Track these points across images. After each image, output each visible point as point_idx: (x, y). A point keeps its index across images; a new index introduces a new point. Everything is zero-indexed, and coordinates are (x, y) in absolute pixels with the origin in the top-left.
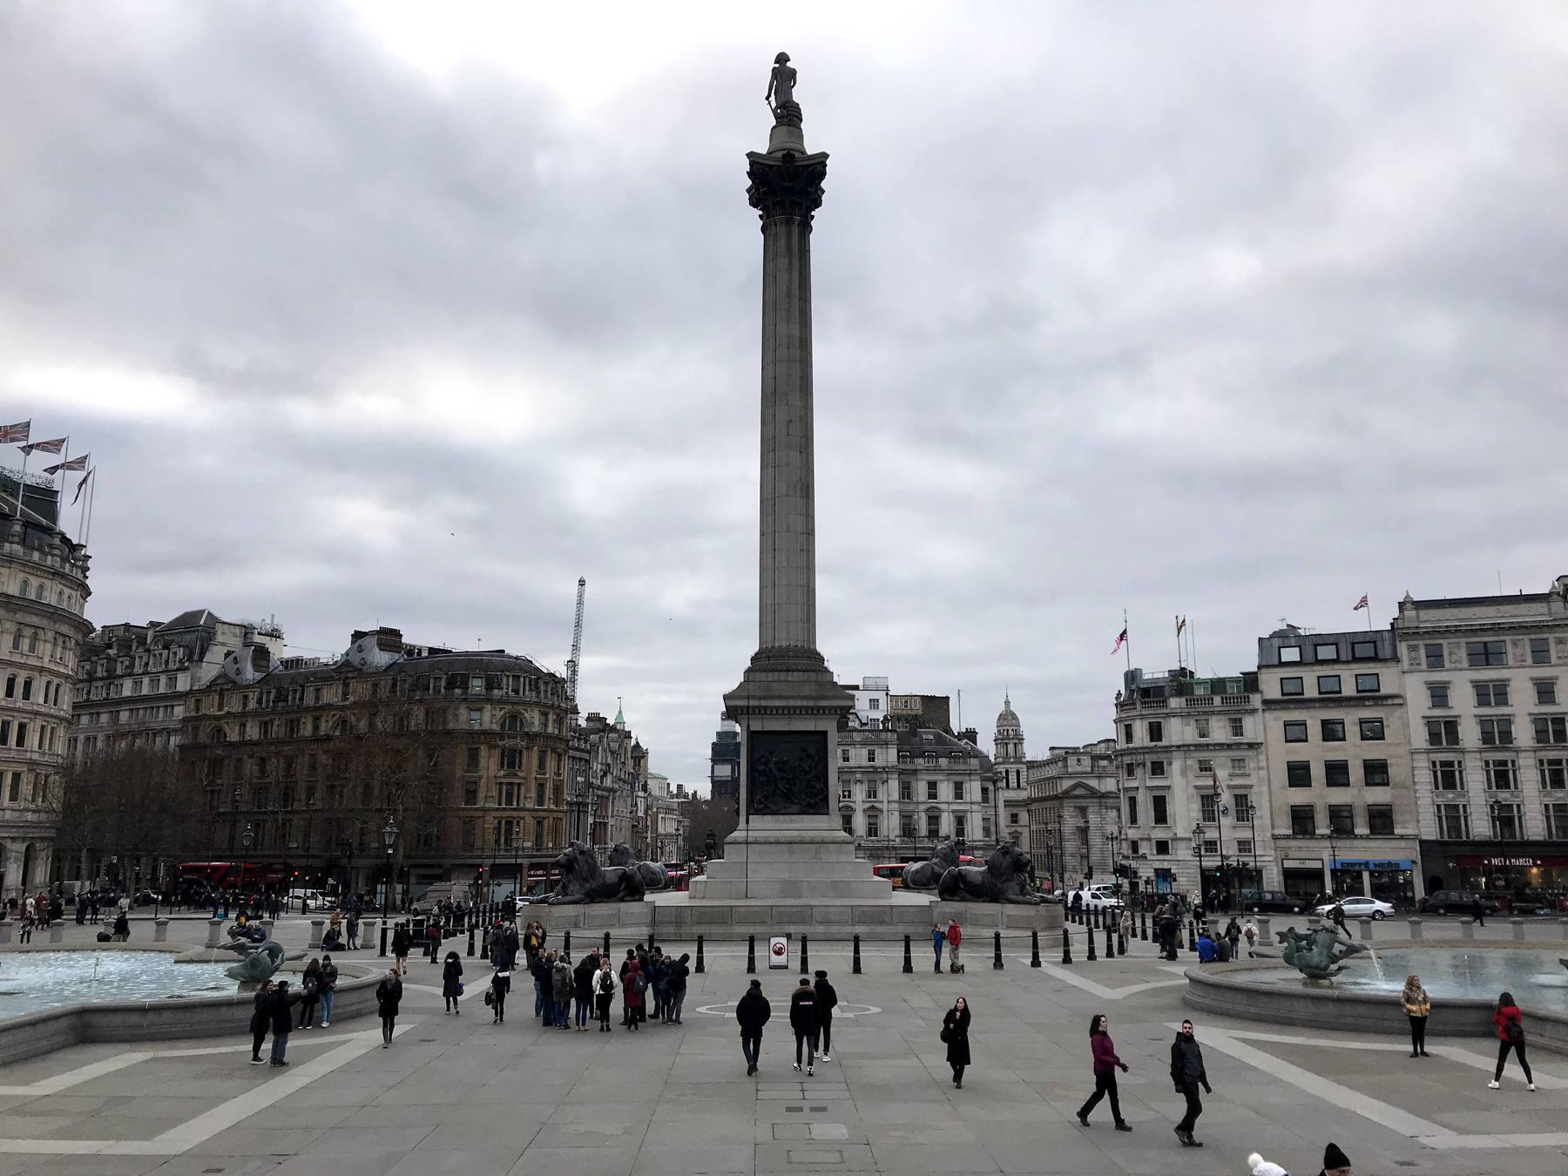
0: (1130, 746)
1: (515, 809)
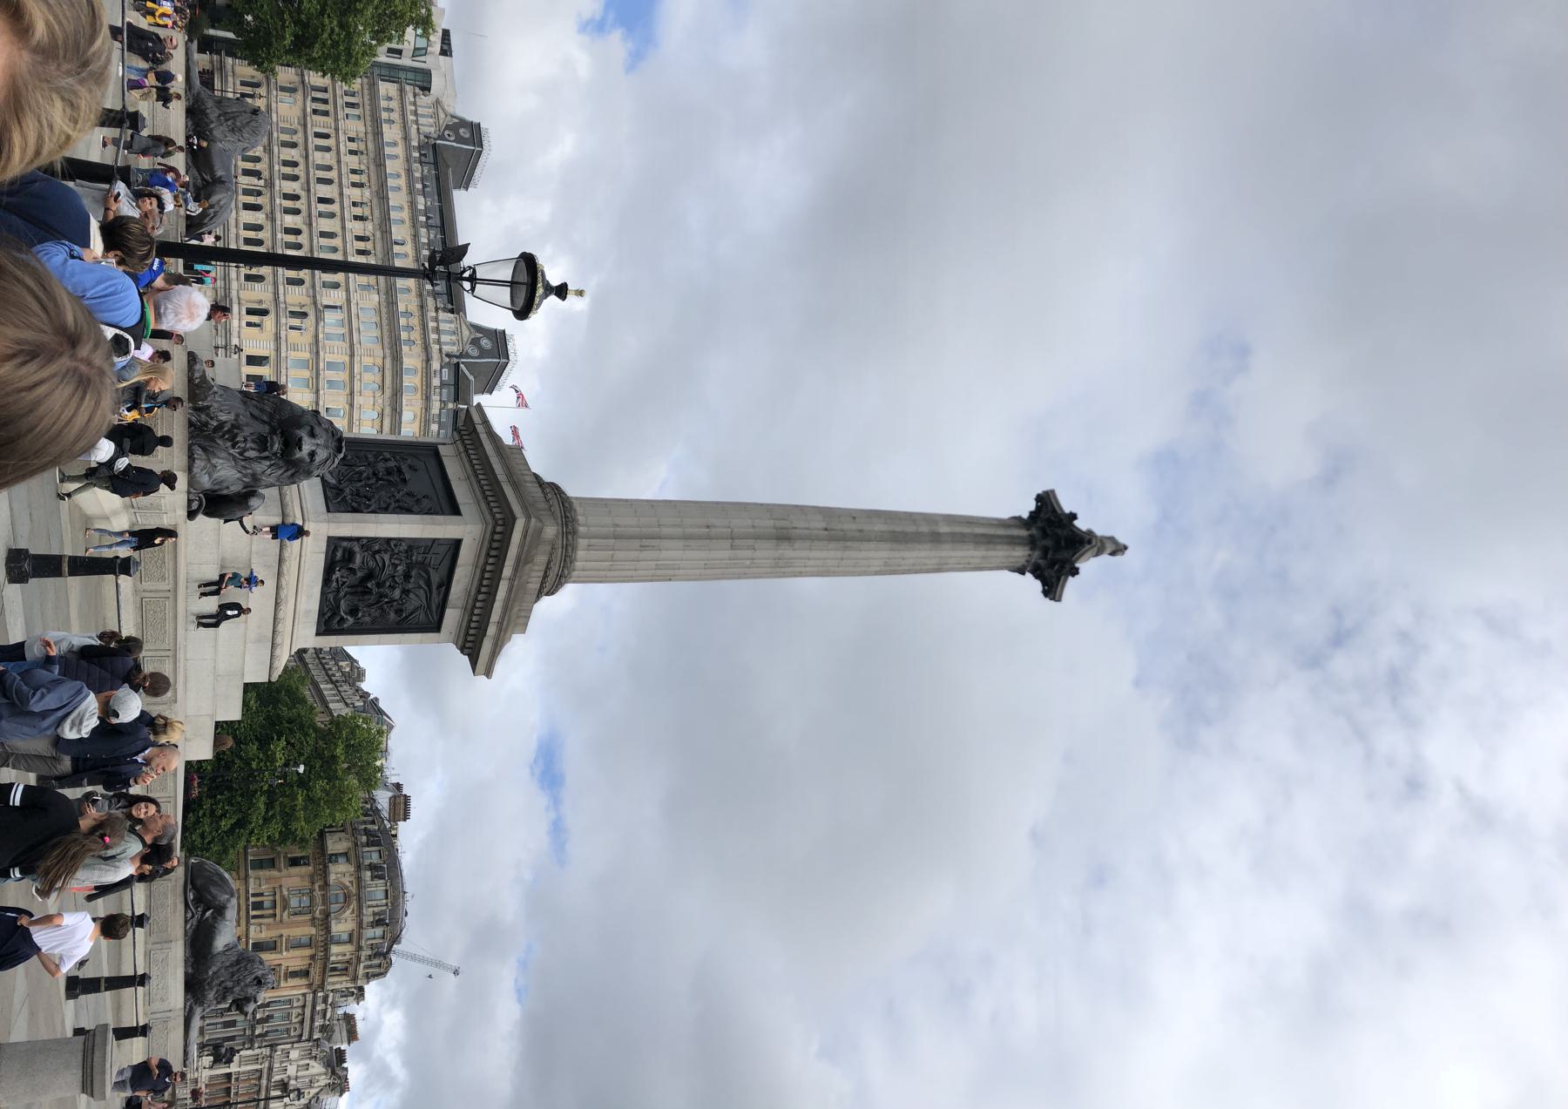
1: (248, 912)
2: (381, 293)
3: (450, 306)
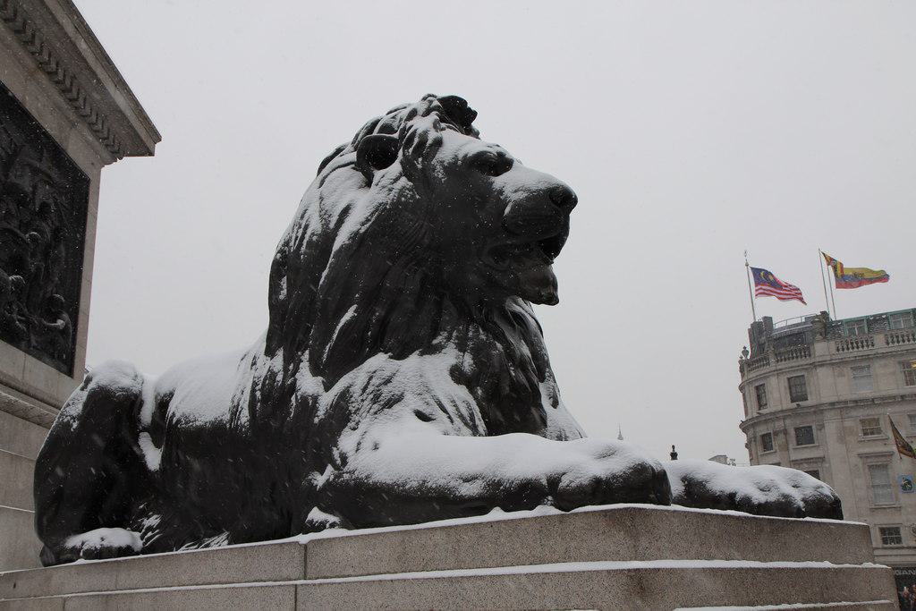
0: (763, 411)
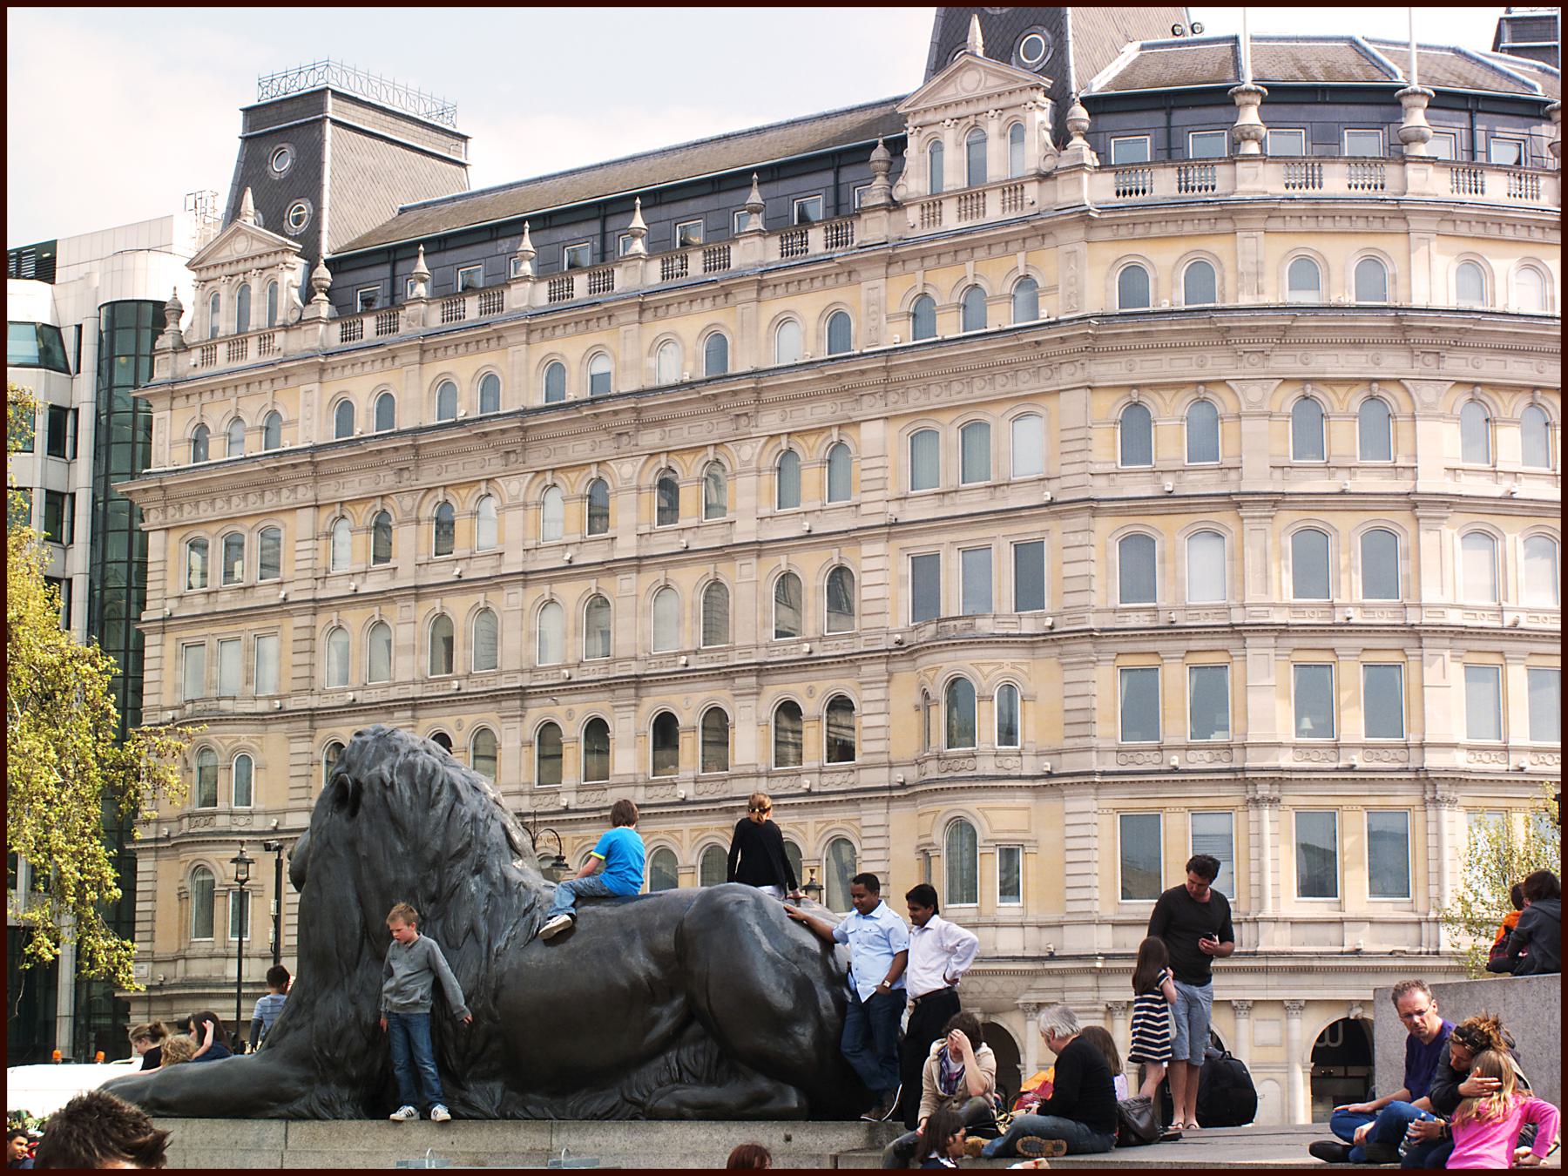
2: (856, 415)
3: (879, 154)
